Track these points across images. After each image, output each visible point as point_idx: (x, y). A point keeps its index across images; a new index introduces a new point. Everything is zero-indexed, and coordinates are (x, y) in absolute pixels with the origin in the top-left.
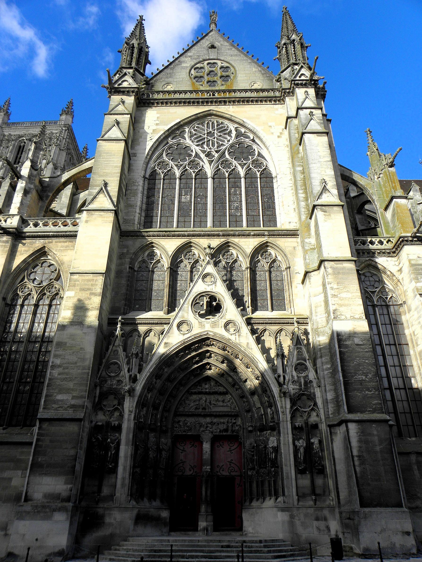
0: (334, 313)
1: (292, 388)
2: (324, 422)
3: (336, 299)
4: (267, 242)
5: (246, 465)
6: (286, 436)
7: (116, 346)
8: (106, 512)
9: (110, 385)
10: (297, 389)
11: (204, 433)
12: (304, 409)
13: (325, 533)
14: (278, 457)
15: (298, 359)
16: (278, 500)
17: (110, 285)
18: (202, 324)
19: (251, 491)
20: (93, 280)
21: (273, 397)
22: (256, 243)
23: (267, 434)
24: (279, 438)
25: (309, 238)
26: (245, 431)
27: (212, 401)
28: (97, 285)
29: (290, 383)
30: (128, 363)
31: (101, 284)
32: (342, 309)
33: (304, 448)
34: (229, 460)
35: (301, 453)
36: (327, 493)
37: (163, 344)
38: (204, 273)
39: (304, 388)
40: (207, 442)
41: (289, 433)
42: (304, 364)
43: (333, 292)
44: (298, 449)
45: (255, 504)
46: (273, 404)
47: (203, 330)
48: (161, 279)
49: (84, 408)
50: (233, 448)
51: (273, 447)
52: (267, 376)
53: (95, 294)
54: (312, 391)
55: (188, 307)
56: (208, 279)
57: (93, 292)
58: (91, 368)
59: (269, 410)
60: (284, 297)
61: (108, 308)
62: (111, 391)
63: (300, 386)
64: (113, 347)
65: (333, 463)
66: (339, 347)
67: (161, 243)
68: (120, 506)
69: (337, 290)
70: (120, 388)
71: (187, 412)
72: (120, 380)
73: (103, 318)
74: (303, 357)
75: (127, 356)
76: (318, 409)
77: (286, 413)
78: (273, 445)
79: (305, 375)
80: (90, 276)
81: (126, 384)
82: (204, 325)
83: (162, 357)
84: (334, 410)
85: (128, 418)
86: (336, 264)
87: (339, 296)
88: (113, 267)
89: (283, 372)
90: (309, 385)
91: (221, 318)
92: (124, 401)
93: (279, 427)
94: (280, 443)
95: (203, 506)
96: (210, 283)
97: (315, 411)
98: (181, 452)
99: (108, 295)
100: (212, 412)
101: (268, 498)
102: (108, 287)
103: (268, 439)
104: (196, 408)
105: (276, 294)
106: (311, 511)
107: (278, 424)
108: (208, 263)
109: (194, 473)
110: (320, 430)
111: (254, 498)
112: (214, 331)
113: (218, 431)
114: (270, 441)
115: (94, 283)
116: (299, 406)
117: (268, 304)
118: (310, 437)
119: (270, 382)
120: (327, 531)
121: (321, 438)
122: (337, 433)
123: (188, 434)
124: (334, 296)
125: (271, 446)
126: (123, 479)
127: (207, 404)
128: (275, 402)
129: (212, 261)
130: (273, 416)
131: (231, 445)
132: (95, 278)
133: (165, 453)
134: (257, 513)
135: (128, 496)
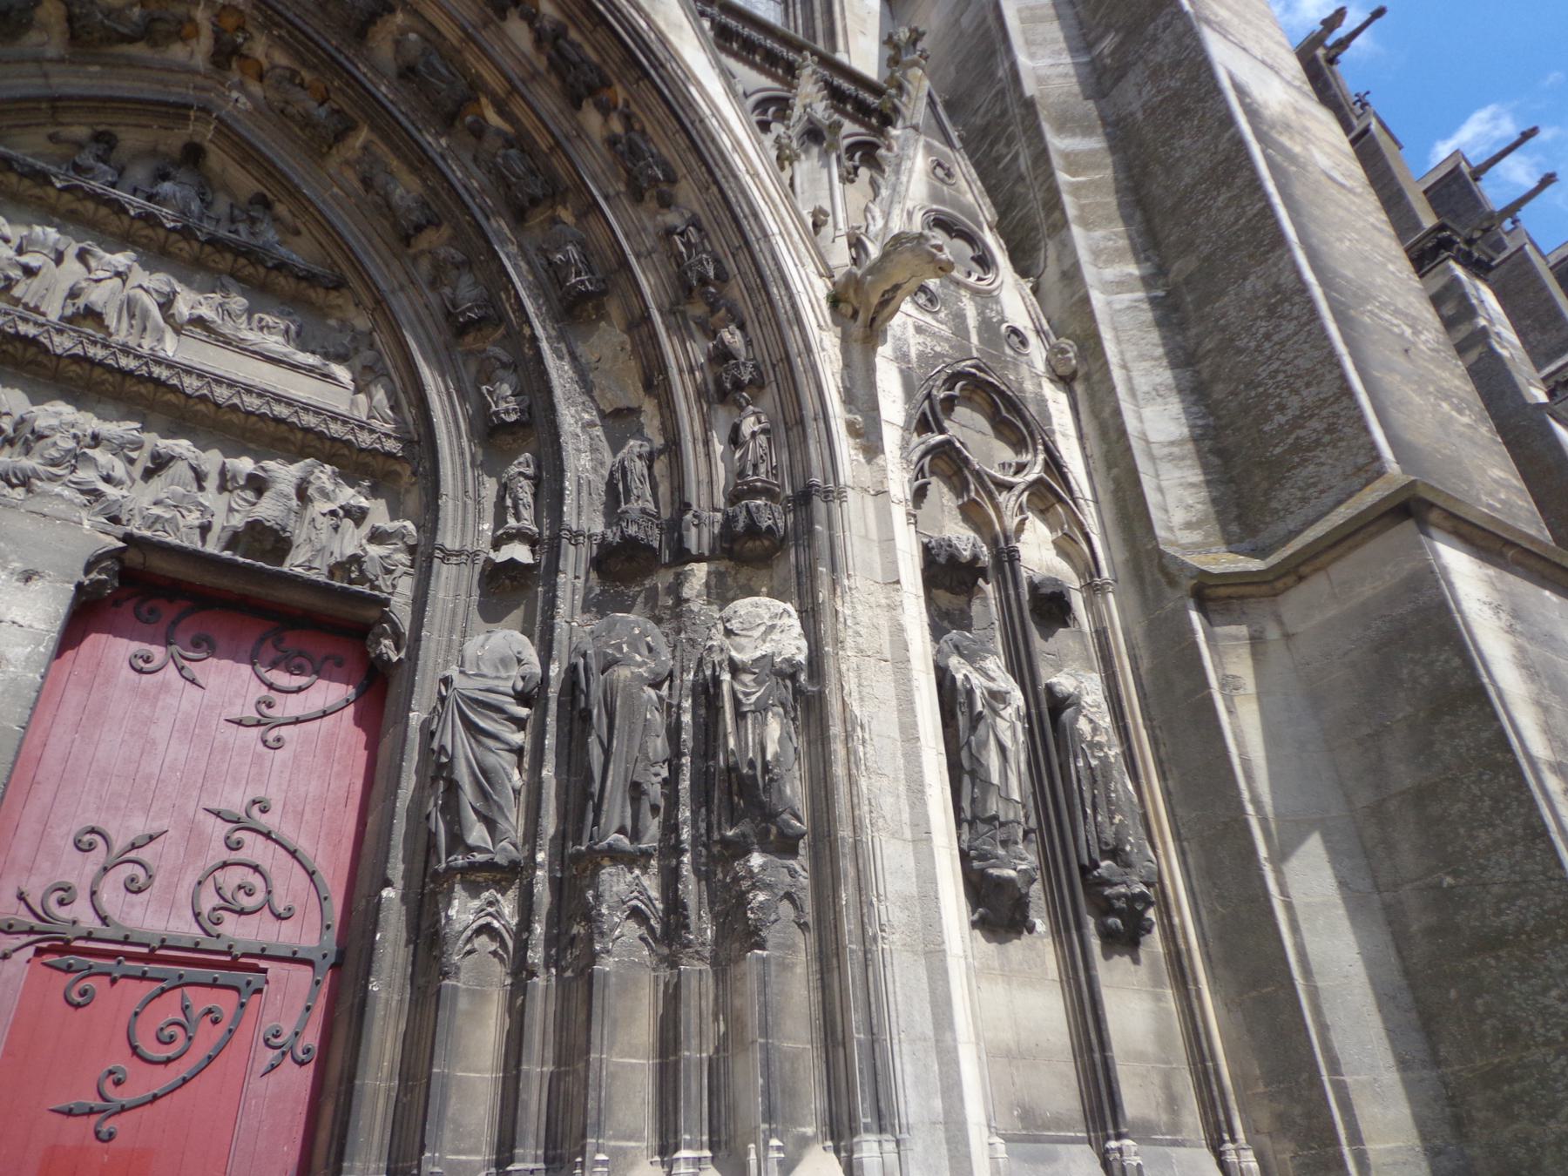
15: (935, 196)
34: (236, 801)
35: (1002, 749)
40: (28, 577)
78: (766, 648)
100: (170, 365)
113: (194, 518)
131: (281, 678)
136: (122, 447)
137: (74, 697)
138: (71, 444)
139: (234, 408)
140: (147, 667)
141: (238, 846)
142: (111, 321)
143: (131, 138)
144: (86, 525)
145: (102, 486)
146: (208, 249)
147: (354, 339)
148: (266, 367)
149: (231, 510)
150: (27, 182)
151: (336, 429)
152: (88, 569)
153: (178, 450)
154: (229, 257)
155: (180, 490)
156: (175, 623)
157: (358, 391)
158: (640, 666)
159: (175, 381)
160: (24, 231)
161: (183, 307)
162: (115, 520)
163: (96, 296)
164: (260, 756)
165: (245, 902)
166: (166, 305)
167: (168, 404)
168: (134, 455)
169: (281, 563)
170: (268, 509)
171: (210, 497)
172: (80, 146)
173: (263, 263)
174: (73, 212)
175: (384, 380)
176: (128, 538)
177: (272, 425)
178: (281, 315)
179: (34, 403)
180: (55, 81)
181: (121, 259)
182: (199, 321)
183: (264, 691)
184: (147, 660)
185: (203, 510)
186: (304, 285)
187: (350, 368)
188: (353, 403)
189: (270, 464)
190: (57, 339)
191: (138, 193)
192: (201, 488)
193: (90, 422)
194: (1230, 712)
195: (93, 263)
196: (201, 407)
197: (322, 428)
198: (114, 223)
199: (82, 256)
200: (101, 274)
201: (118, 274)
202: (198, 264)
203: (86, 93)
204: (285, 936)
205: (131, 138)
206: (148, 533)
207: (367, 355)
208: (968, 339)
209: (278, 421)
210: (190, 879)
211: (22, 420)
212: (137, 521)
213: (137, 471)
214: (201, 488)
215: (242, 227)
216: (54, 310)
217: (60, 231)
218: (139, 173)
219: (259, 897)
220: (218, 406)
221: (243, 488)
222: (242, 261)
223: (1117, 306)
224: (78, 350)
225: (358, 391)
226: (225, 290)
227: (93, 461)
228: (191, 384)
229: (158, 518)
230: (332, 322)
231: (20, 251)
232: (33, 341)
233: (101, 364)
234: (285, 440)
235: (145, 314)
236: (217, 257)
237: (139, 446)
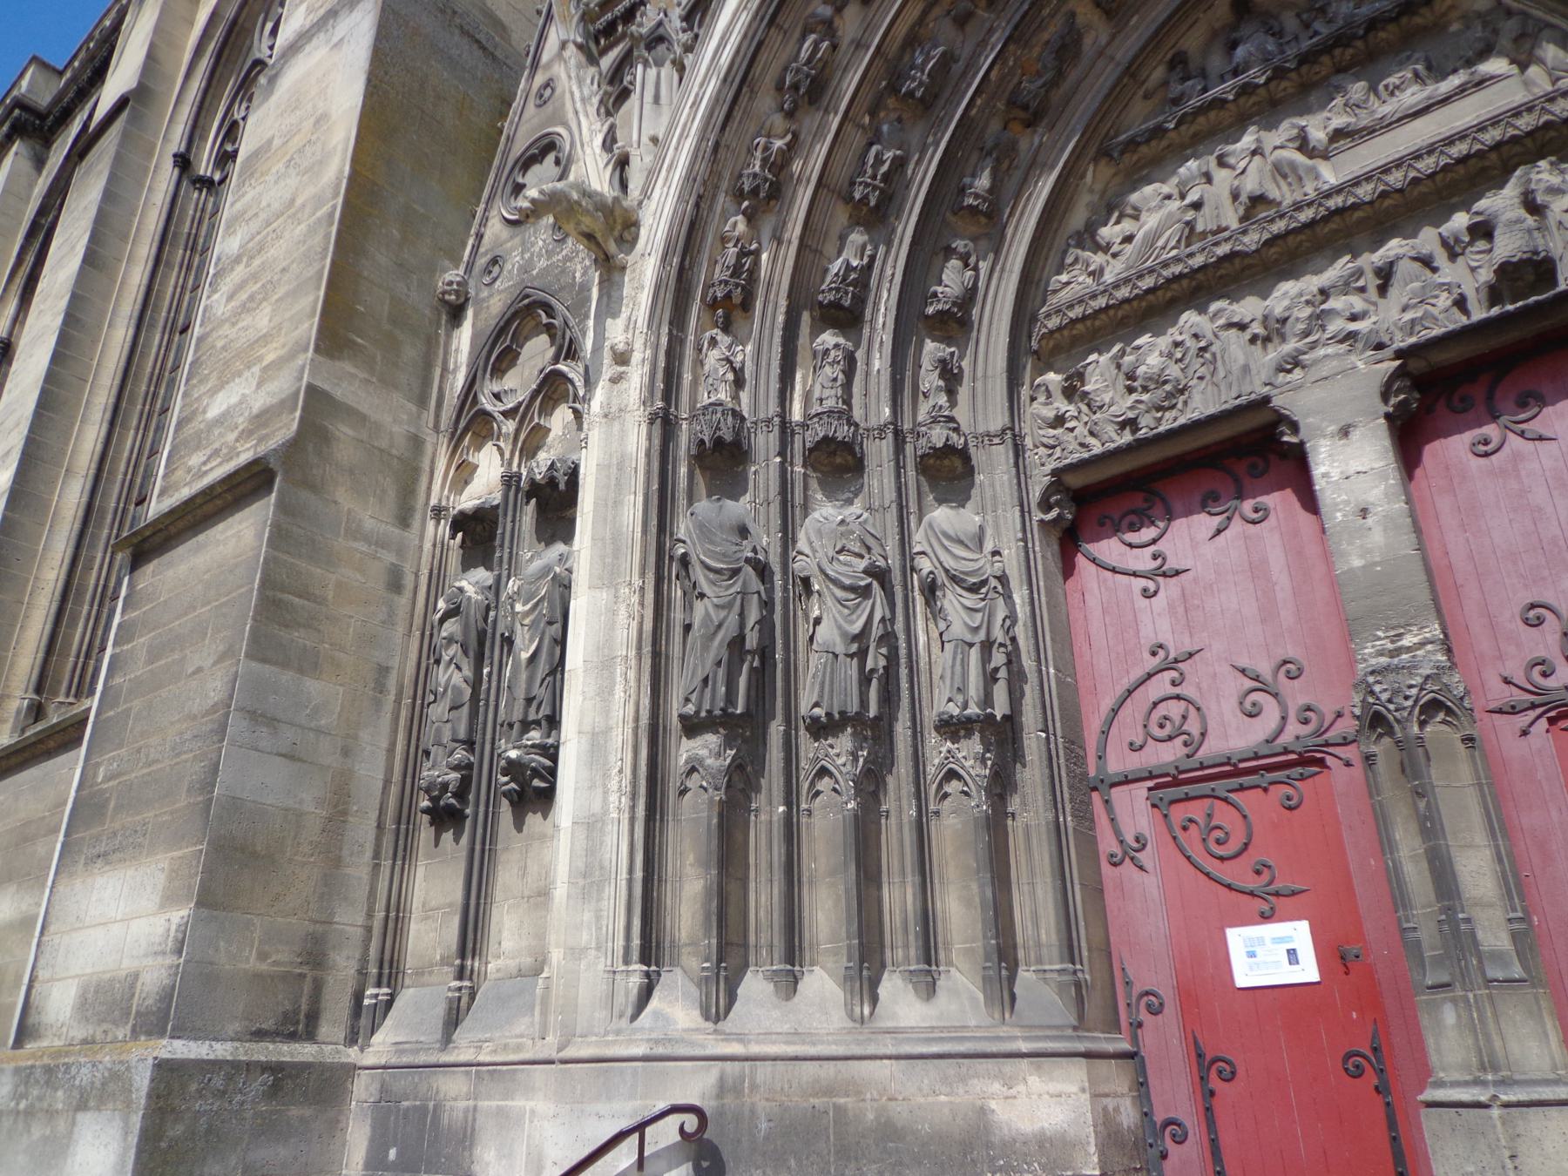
8: (484, 1104)
40: (1345, 432)
68: (570, 1053)
71: (1116, 286)
95: (1449, 1016)
98: (1146, 594)
100: (1338, 190)
113: (1444, 300)
133: (971, 600)
135: (626, 962)
136: (1347, 284)
137: (1444, 504)
138: (1308, 311)
139: (1415, 181)
140: (1489, 448)
142: (1274, 193)
143: (1192, 42)
144: (1361, 365)
145: (1353, 326)
146: (1304, 69)
147: (1485, 24)
148: (1419, 123)
149: (1473, 270)
150: (1153, 143)
151: (1526, 123)
152: (1385, 396)
153: (1392, 253)
154: (1325, 59)
155: (1416, 285)
156: (1490, 398)
157: (1523, 67)
159: (1351, 200)
160: (1175, 180)
161: (1318, 135)
162: (1380, 346)
163: (1250, 185)
166: (1303, 144)
167: (1361, 221)
168: (1361, 283)
169: (1555, 283)
170: (1507, 246)
171: (1449, 272)
172: (1165, 84)
173: (1355, 37)
174: (1195, 135)
175: (1546, 33)
176: (1399, 354)
177: (1461, 170)
178: (1401, 65)
179: (1265, 298)
180: (1118, 56)
181: (1248, 140)
182: (1338, 135)
184: (1486, 443)
185: (1447, 287)
186: (1404, 20)
187: (1501, 54)
188: (1527, 84)
189: (1482, 204)
190: (1246, 239)
191: (1226, 77)
192: (1435, 270)
193: (1311, 283)
195: (1232, 160)
196: (1388, 202)
197: (1511, 132)
198: (1226, 116)
199: (1222, 162)
200: (1242, 164)
201: (1254, 153)
202: (1305, 88)
203: (1140, 44)
205: (1192, 42)
206: (1413, 340)
207: (1510, 27)
209: (1463, 160)
211: (1266, 318)
212: (1398, 336)
213: (1372, 293)
214: (1435, 270)
215: (1318, 25)
216: (1231, 220)
217: (1197, 158)
218: (1216, 62)
220: (1400, 191)
221: (1471, 243)
222: (1337, 52)
224: (1266, 236)
225: (1523, 67)
226: (1339, 89)
227: (1331, 313)
228: (1365, 192)
229: (1413, 322)
230: (1455, 27)
231: (1183, 197)
232: (1232, 255)
233: (1288, 233)
234: (1484, 170)
235: (1293, 166)
236: (1317, 68)
237: (1359, 273)
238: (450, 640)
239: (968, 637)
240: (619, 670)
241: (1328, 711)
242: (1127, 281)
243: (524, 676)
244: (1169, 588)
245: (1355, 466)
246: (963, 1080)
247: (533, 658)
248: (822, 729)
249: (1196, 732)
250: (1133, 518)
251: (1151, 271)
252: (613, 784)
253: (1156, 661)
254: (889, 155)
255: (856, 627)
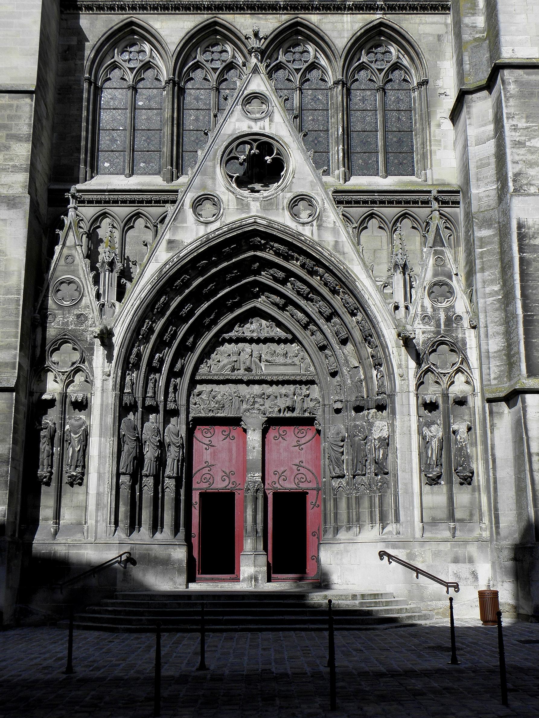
0: (514, 181)
1: (421, 331)
2: (479, 394)
3: (522, 151)
4: (381, 24)
5: (327, 470)
6: (406, 418)
7: (70, 248)
9: (63, 323)
10: (431, 332)
11: (248, 414)
12: (442, 369)
13: (469, 582)
14: (390, 455)
15: (435, 275)
16: (386, 530)
17: (47, 118)
18: (244, 202)
19: (336, 514)
20: (11, 106)
21: (384, 347)
22: (357, 26)
23: (370, 416)
24: (393, 422)
25: (473, 14)
26: (326, 409)
27: (263, 356)
28: (19, 117)
29: (418, 320)
30: (96, 281)
31: (28, 115)
32: (532, 172)
33: (439, 440)
34: (297, 461)
35: (432, 449)
36: (476, 517)
37: (164, 244)
38: (246, 93)
39: (444, 331)
40: (254, 430)
41: (411, 413)
42: (447, 284)
43: (517, 136)
44: (428, 442)
45: (342, 535)
46: (384, 361)
47: (244, 216)
48: (154, 105)
49: (15, 369)
50: (303, 441)
51: (379, 438)
52: (372, 307)
53: (18, 138)
54: (460, 336)
55: (214, 167)
56: (255, 105)
57: (13, 132)
58: (22, 291)
59: (375, 372)
60: (412, 146)
61: (46, 168)
62: (65, 335)
63: (438, 326)
64: (62, 248)
65: (491, 466)
66: (521, 250)
67: (151, 23)
69: (525, 132)
70: (83, 331)
71: (215, 375)
72: (82, 314)
73: (38, 188)
74: (446, 269)
75: (93, 268)
76: (470, 369)
77: (408, 376)
78: (380, 435)
79: (448, 305)
80: (4, 97)
81: (94, 322)
82: (248, 205)
83: (165, 270)
84: (501, 371)
85: (103, 387)
86: (528, 74)
87: (528, 144)
88: (51, 78)
89: (405, 299)
90: (454, 325)
91: (283, 190)
92: (92, 354)
93: (393, 402)
94: (393, 431)
95: (249, 541)
96: (258, 116)
97: (463, 373)
99: (45, 139)
100: (264, 375)
101: (368, 526)
102: (44, 122)
103: (371, 425)
104: (233, 370)
105: (395, 139)
106: (446, 547)
107: (392, 396)
108: (255, 70)
109: (231, 485)
110: (470, 408)
111: (341, 527)
112: (270, 218)
113: (277, 409)
114: (374, 428)
115: (14, 113)
116: (434, 365)
117: (377, 162)
118: (452, 421)
119: (380, 319)
120: (471, 579)
121: (470, 421)
122: (503, 413)
123: (219, 415)
124: (519, 144)
125: (376, 437)
126: (99, 494)
127: (255, 362)
128: (387, 357)
129: (262, 67)
130: (383, 382)
132: (15, 102)
134: (348, 552)
141: (299, 470)
158: (360, 436)
162: (265, 414)
164: (299, 452)
165: (303, 480)
176: (267, 417)
183: (297, 439)
194: (491, 433)
204: (310, 485)
206: (270, 415)
208: (440, 327)
210: (293, 477)
219: (305, 479)
223: (488, 303)
238: (45, 437)
239: (175, 458)
240: (108, 459)
241: (238, 483)
242: (217, 375)
243: (76, 454)
244: (211, 450)
245: (254, 438)
246: (168, 549)
247: (79, 451)
248: (147, 476)
249: (212, 482)
250: (206, 430)
251: (223, 375)
252: (106, 486)
253: (206, 465)
254: (174, 329)
255: (156, 455)
